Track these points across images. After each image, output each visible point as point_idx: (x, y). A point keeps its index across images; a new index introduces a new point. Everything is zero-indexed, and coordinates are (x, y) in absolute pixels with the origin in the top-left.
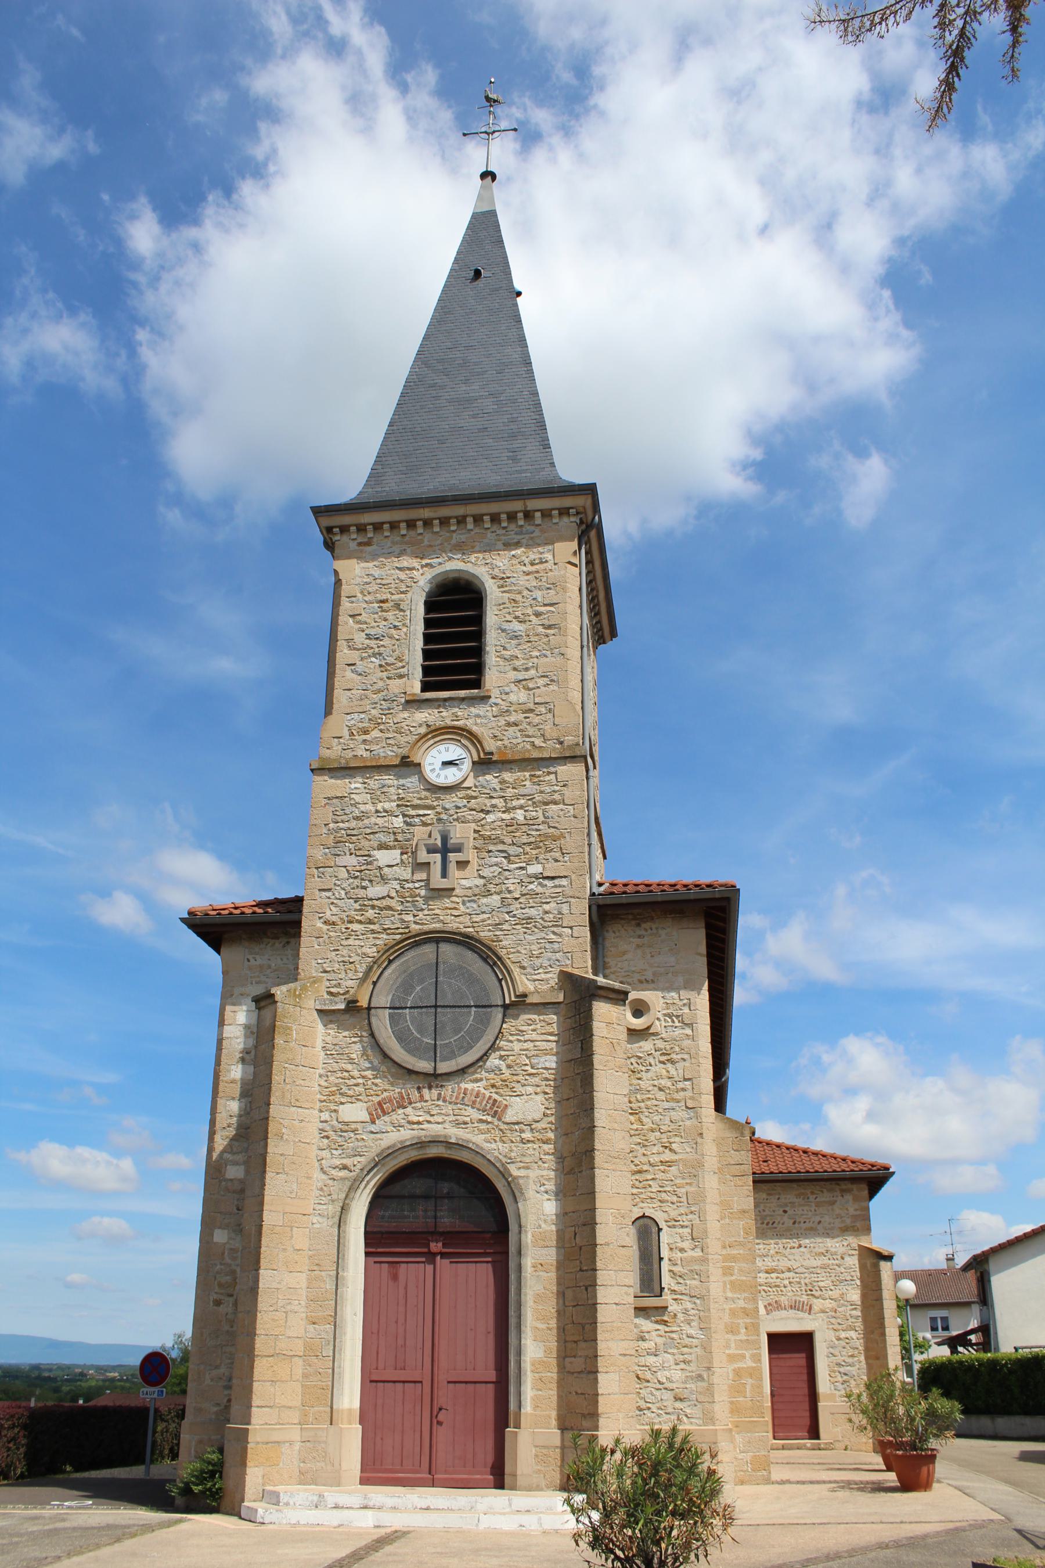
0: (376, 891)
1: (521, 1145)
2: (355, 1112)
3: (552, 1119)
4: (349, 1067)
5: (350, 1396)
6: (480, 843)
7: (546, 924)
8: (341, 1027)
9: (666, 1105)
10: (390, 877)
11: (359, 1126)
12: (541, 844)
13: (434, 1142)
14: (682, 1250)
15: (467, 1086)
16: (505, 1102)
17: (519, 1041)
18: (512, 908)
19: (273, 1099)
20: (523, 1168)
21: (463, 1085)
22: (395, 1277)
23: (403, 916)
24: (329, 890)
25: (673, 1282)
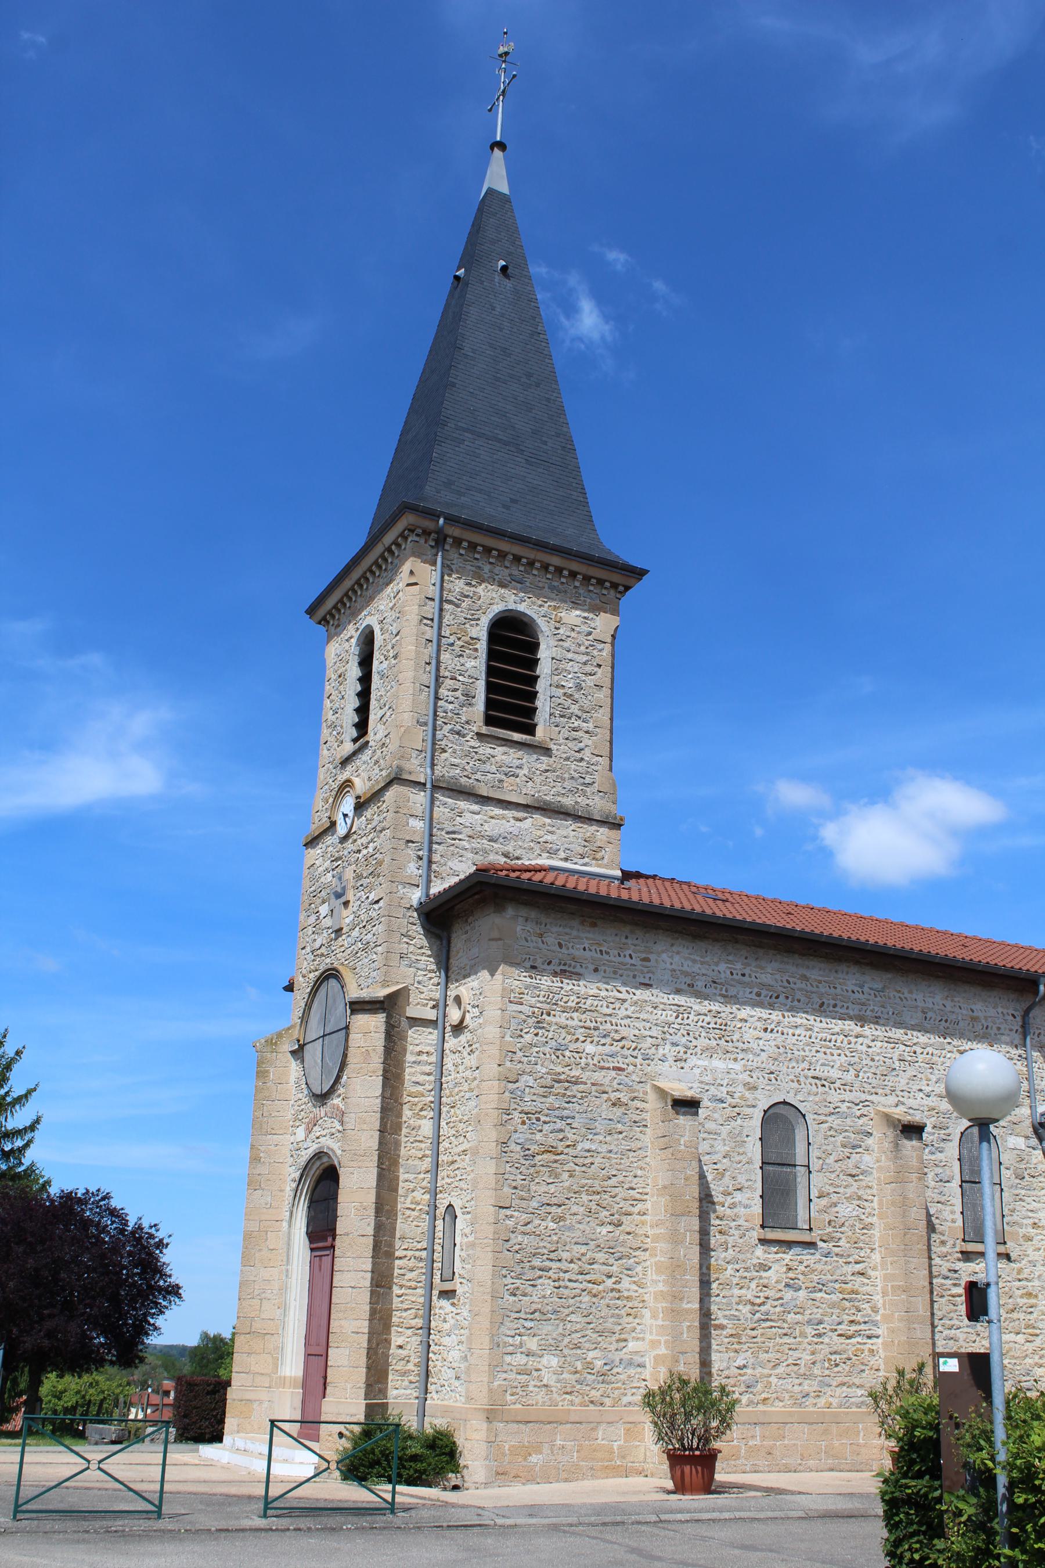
9: (468, 1095)
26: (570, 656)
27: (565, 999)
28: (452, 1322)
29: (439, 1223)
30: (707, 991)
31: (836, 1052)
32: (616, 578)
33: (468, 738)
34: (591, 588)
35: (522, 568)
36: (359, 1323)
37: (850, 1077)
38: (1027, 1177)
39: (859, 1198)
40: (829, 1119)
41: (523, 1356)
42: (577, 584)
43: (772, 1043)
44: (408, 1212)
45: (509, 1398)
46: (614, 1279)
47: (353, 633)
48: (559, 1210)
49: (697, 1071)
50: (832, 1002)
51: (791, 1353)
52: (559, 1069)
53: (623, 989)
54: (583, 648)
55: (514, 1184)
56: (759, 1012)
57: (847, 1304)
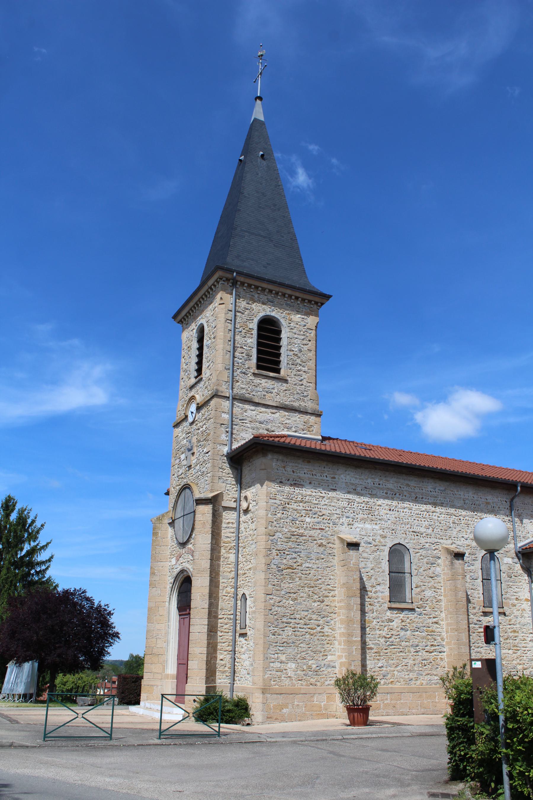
9: (251, 542)
26: (296, 336)
27: (296, 497)
28: (246, 648)
29: (239, 602)
30: (362, 492)
31: (423, 520)
32: (317, 299)
33: (249, 375)
34: (305, 304)
35: (273, 296)
36: (202, 649)
37: (430, 531)
38: (513, 576)
39: (435, 588)
40: (420, 551)
41: (279, 663)
42: (299, 302)
43: (393, 516)
44: (224, 597)
45: (272, 683)
46: (320, 627)
47: (194, 327)
48: (295, 595)
49: (358, 530)
50: (421, 496)
51: (404, 660)
52: (294, 530)
53: (323, 492)
54: (302, 333)
55: (273, 583)
56: (387, 502)
57: (430, 637)
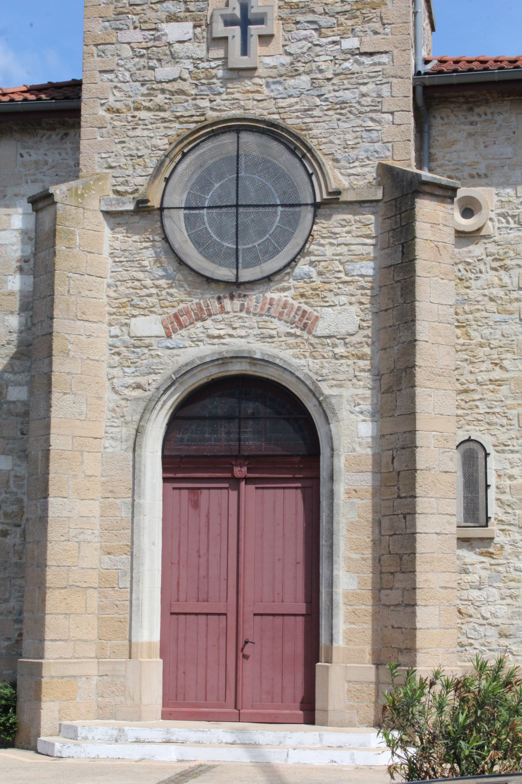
0: (166, 71)
1: (334, 361)
2: (148, 326)
3: (369, 332)
4: (141, 275)
5: (149, 628)
6: (285, 13)
7: (363, 109)
8: (131, 230)
9: (498, 317)
10: (181, 55)
11: (153, 341)
12: (358, 13)
13: (237, 358)
14: (511, 477)
15: (273, 295)
16: (315, 314)
17: (332, 244)
18: (323, 90)
19: (56, 313)
20: (336, 386)
21: (269, 295)
22: (196, 505)
23: (198, 102)
24: (112, 71)
25: (500, 512)
